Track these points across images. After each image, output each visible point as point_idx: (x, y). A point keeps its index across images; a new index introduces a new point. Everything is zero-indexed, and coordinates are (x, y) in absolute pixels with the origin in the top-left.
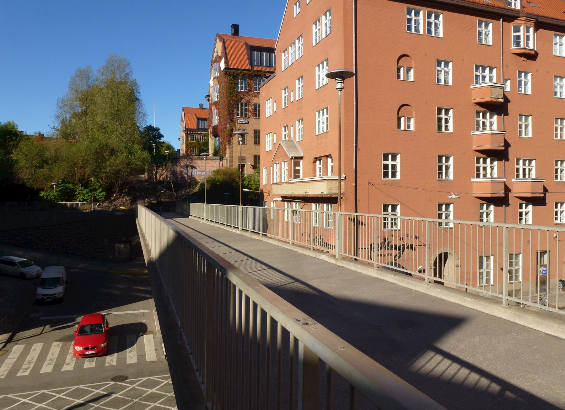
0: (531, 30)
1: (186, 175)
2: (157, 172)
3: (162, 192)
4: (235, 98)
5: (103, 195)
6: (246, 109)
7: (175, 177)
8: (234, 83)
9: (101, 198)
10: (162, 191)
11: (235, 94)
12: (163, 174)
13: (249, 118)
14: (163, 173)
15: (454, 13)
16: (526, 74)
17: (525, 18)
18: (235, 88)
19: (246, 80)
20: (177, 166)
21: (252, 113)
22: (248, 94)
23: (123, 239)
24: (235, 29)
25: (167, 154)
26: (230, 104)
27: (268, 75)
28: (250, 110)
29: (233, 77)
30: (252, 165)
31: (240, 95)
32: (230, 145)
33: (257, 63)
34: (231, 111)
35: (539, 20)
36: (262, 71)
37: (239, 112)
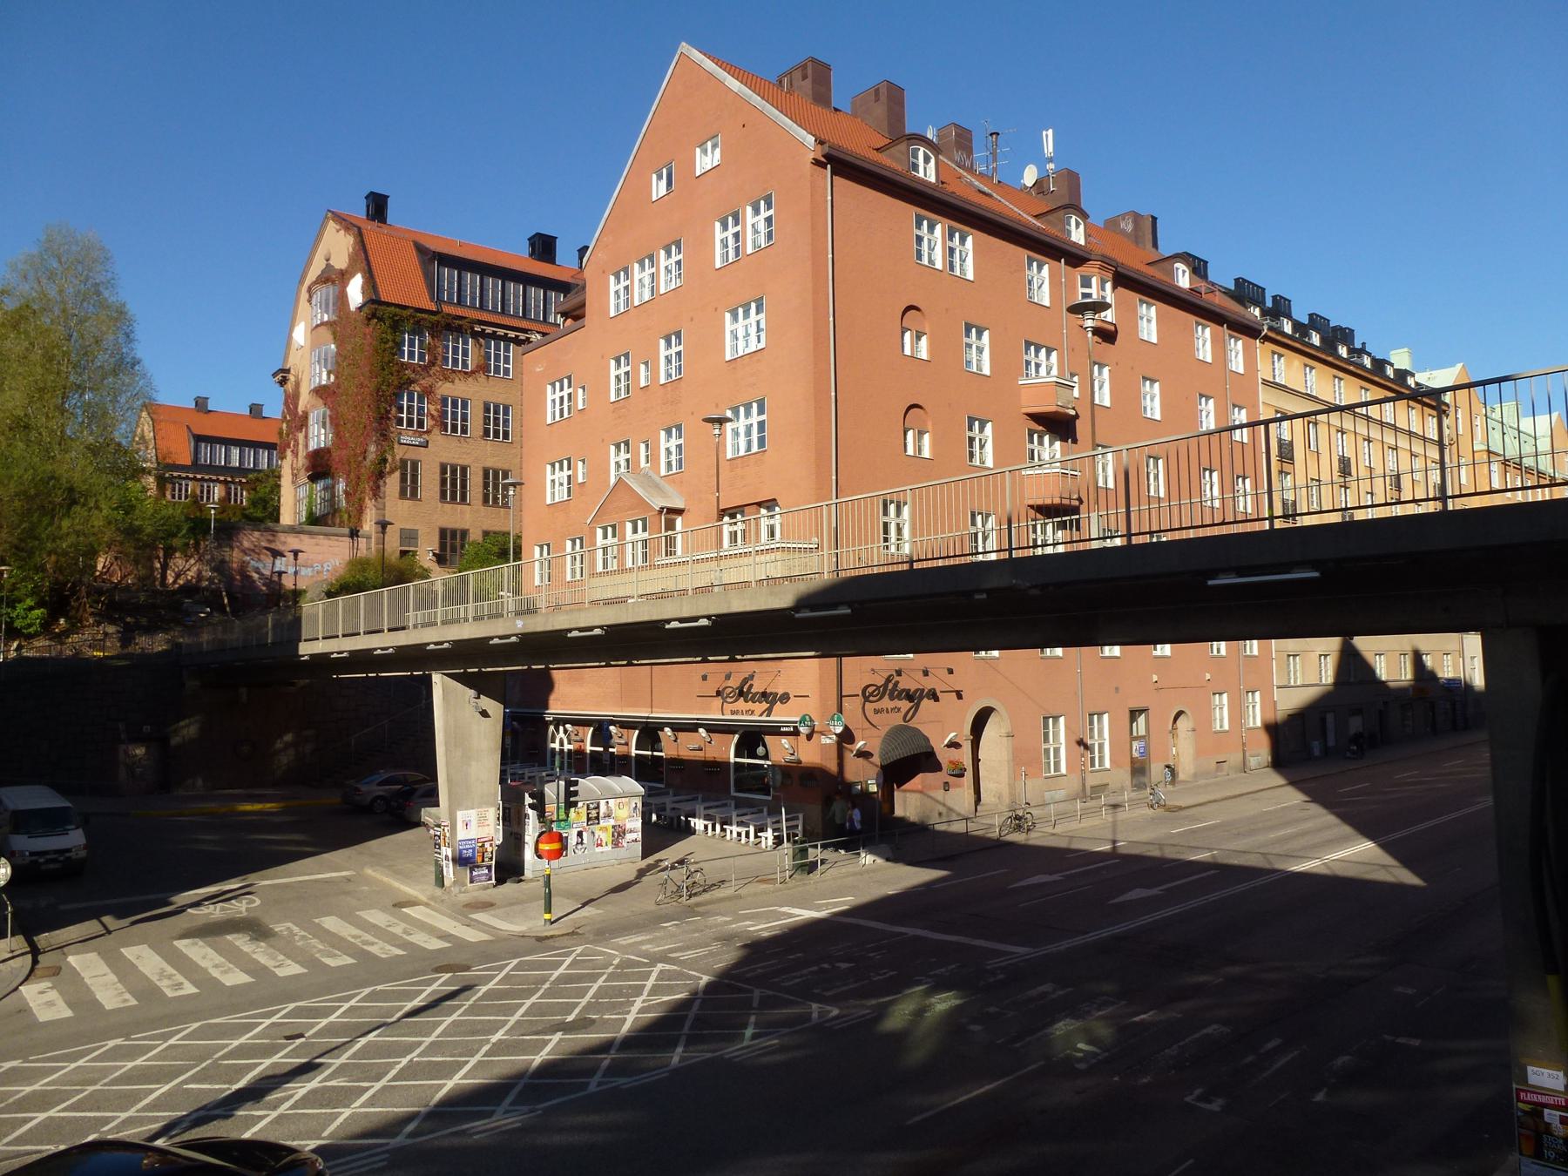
0: (1109, 286)
1: (256, 572)
2: (168, 564)
3: (202, 615)
4: (394, 380)
5: (37, 619)
6: (420, 409)
7: (225, 580)
8: (394, 341)
9: (30, 626)
10: (202, 613)
11: (394, 369)
12: (189, 570)
13: (428, 432)
14: (187, 567)
15: (990, 237)
16: (1101, 366)
17: (1099, 263)
18: (394, 354)
19: (421, 335)
20: (232, 548)
21: (436, 421)
22: (428, 372)
23: (147, 729)
24: (378, 206)
25: (213, 512)
26: (381, 393)
27: (479, 330)
28: (431, 414)
29: (391, 327)
30: (434, 554)
31: (407, 372)
32: (379, 499)
33: (450, 295)
34: (383, 411)
35: (1119, 269)
36: (465, 318)
37: (404, 416)
